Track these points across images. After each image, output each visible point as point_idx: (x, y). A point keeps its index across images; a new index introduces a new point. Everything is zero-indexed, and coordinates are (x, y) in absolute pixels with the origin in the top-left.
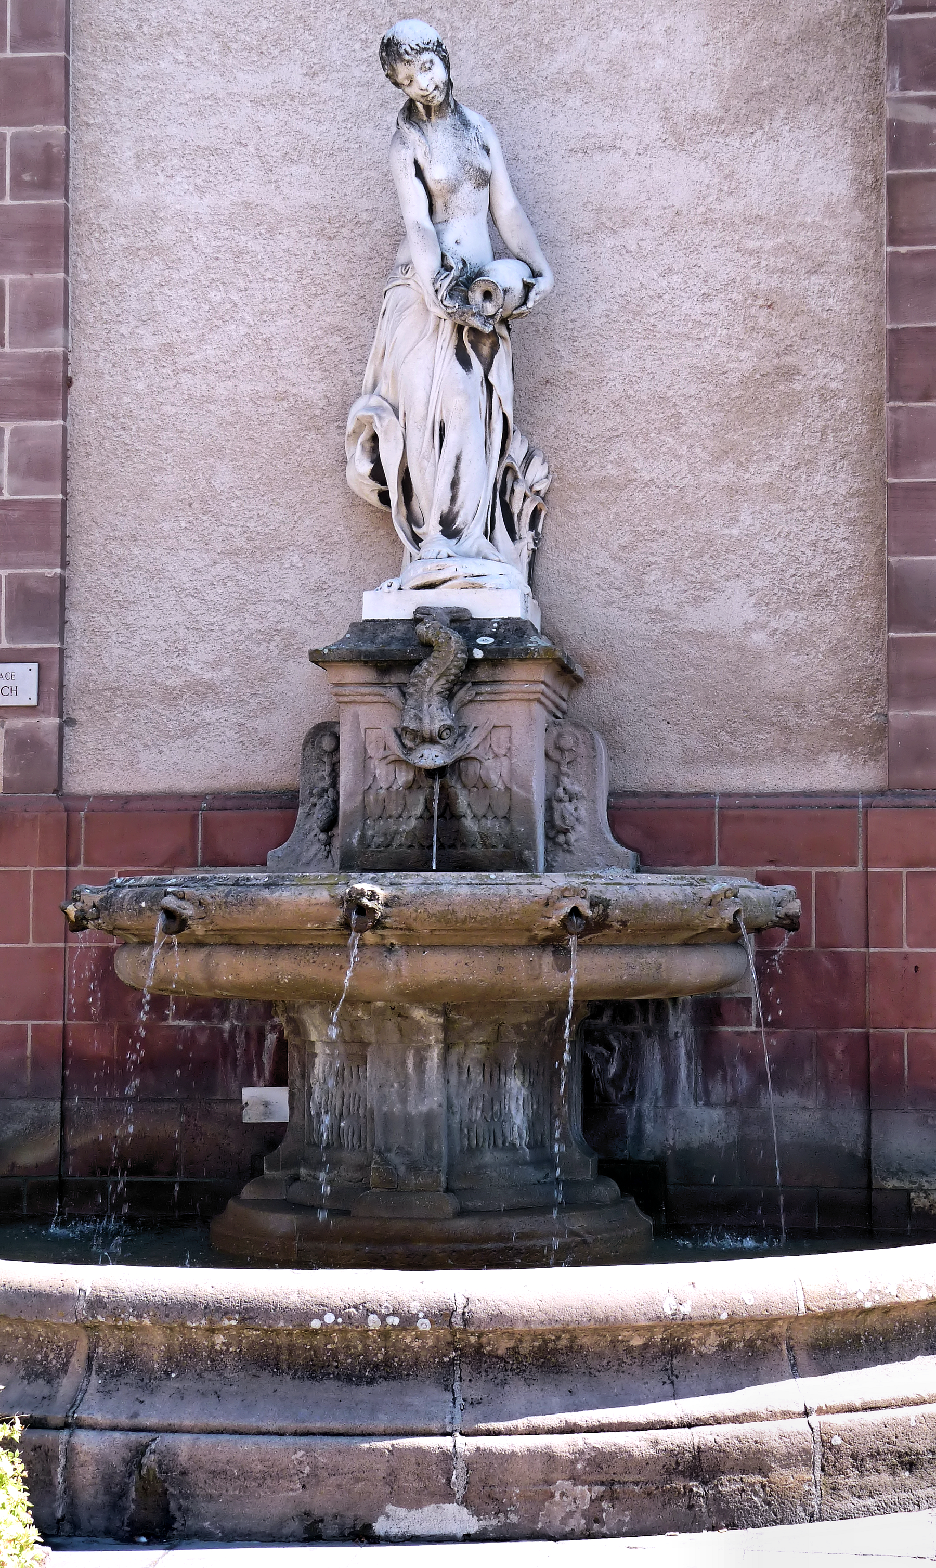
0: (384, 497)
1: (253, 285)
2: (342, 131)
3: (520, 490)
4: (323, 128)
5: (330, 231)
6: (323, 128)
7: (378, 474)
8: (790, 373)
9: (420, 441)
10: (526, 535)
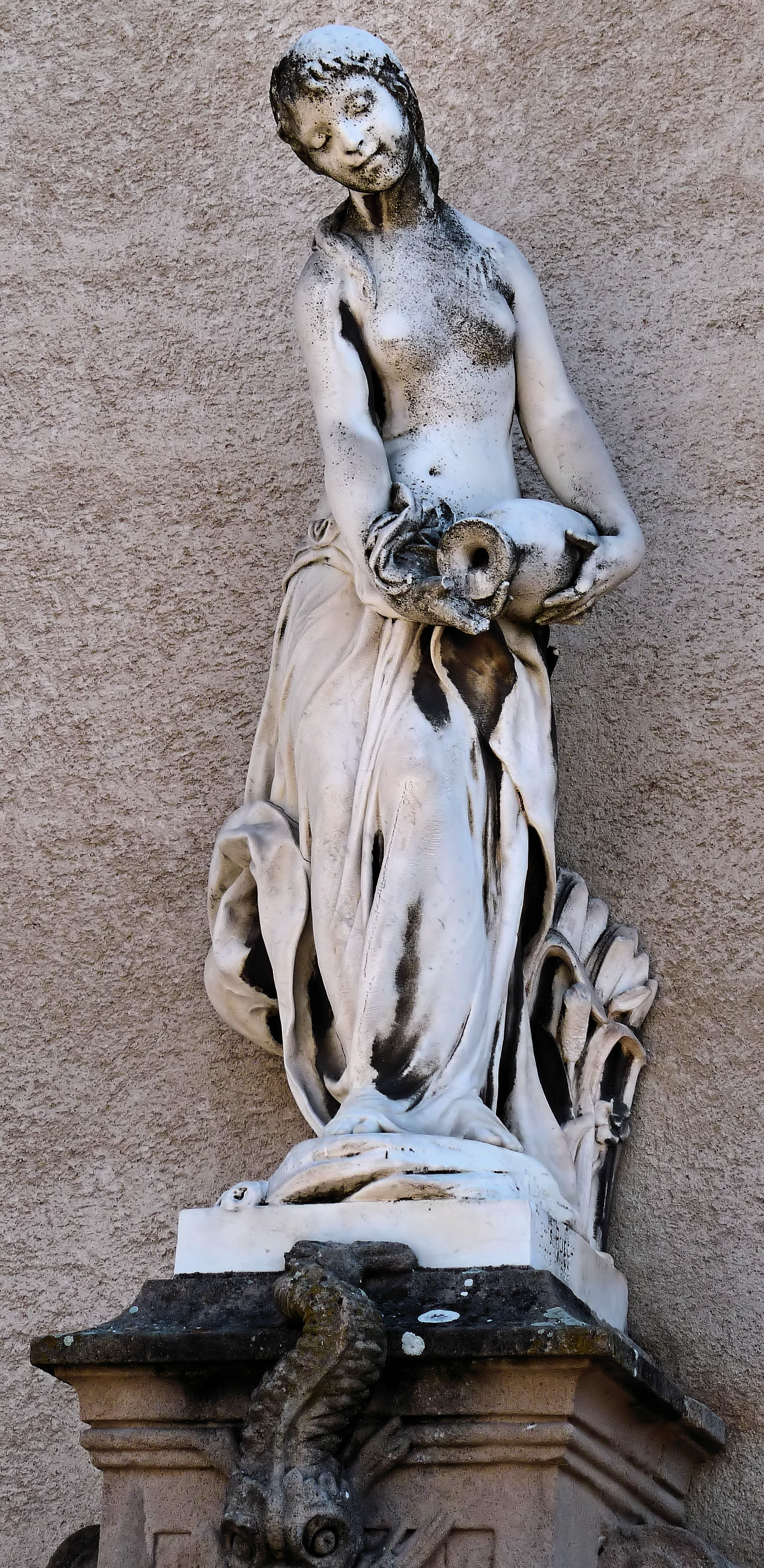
0: (273, 1021)
1: (63, 621)
2: (255, 323)
3: (577, 1007)
4: (220, 320)
5: (221, 509)
6: (220, 320)
7: (257, 971)
10: (593, 1109)
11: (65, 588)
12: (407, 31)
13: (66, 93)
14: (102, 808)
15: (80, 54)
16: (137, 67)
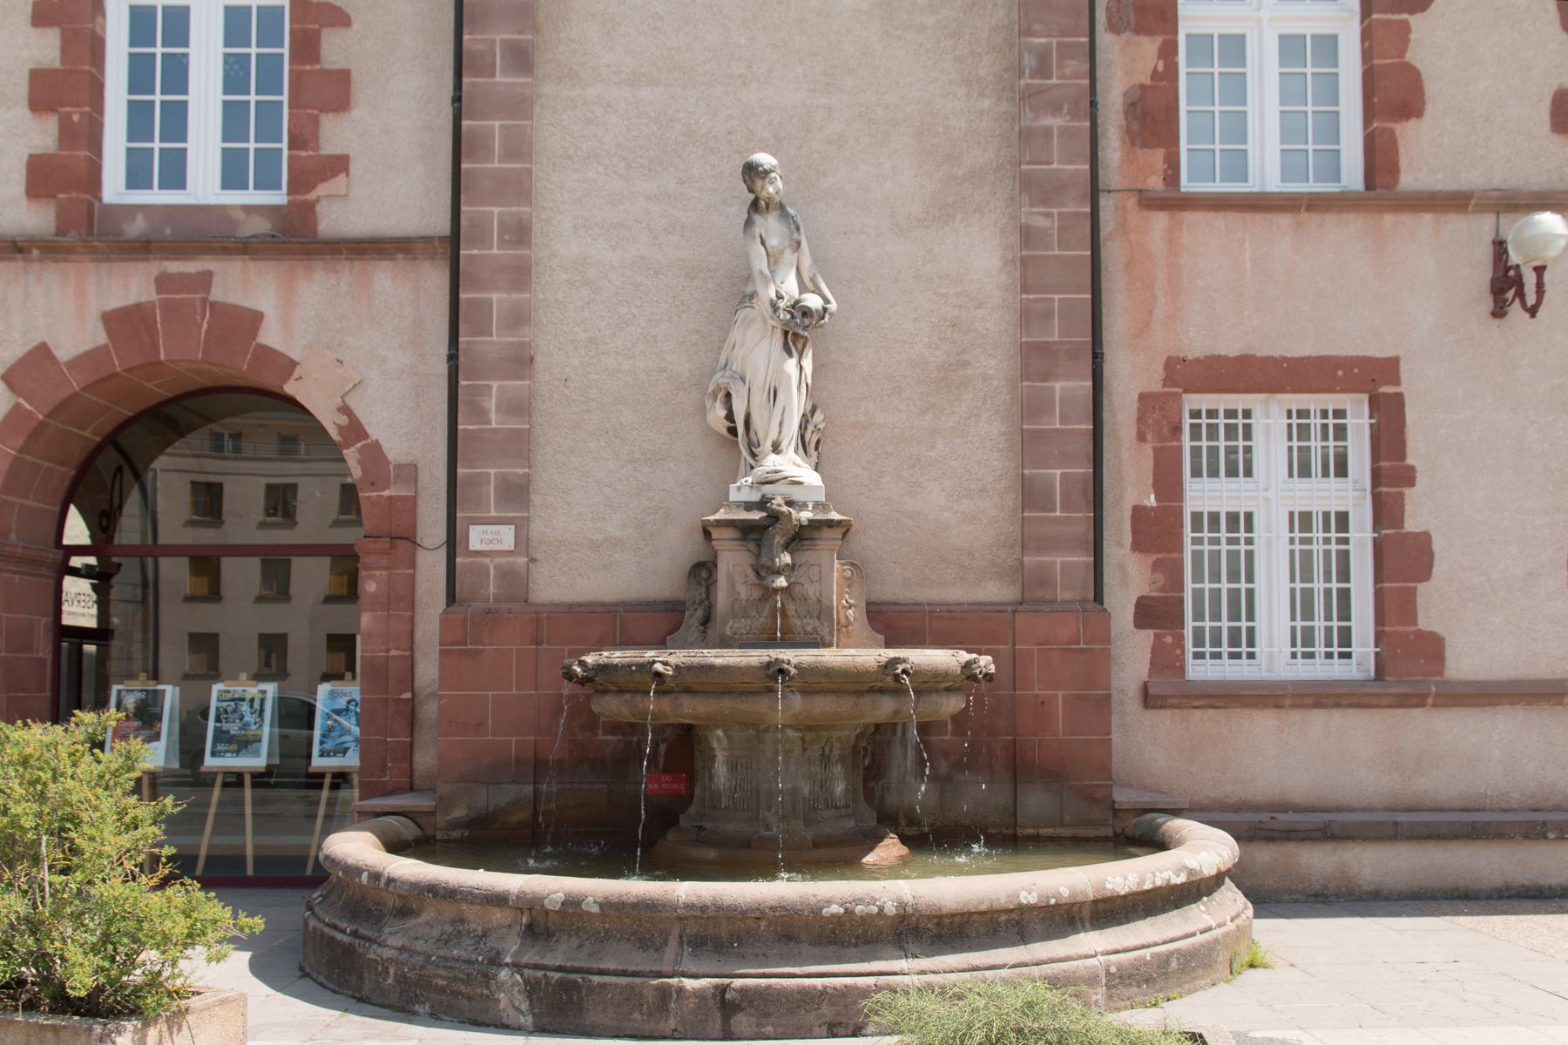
0: (733, 431)
3: (810, 428)
7: (730, 416)
8: (966, 364)
9: (759, 398)
10: (815, 454)
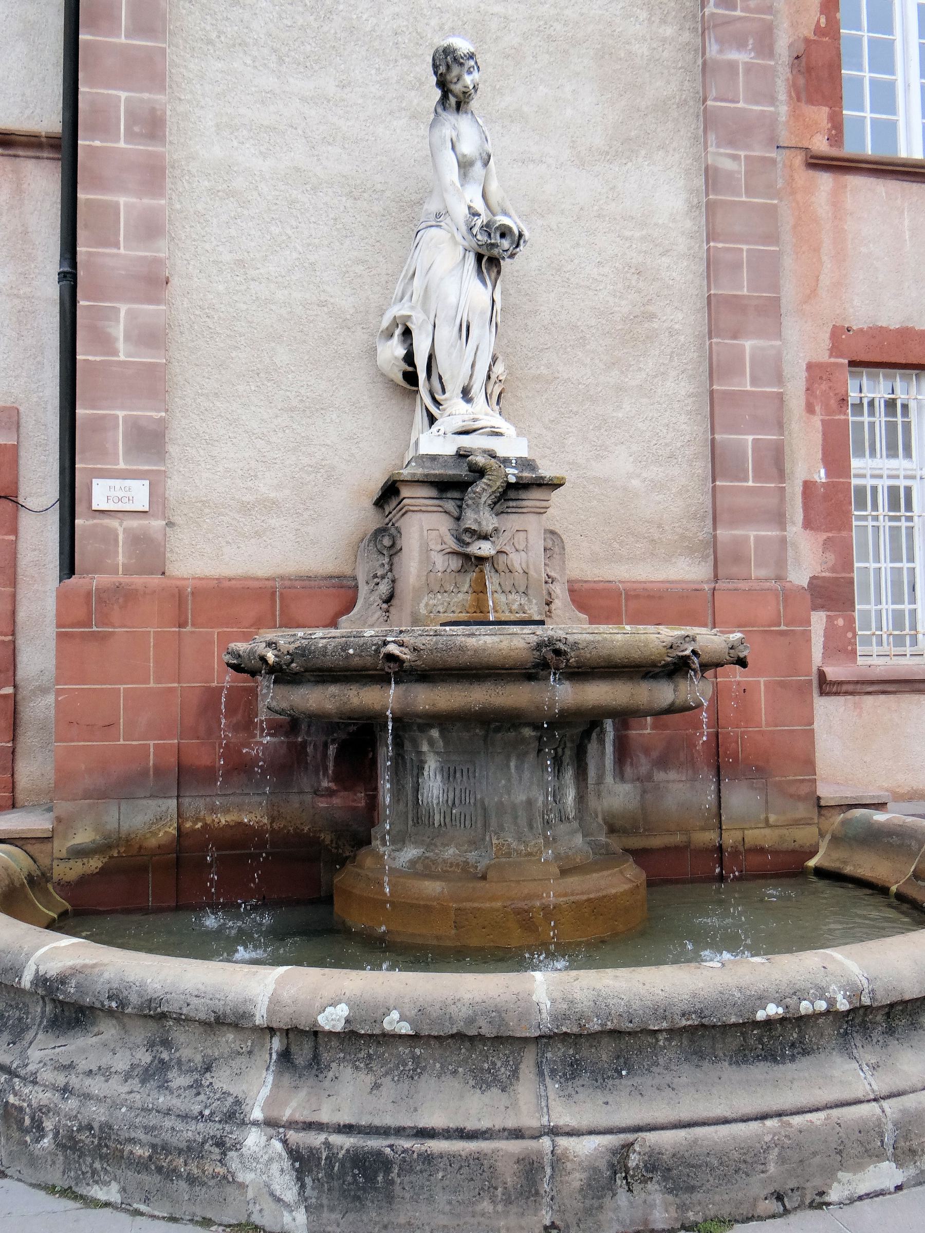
1: (303, 225)
2: (363, 128)
4: (350, 124)
5: (356, 194)
6: (350, 124)
7: (409, 358)
8: (652, 317)
9: (447, 333)
11: (302, 213)
12: (411, 30)
13: (285, 21)
14: (322, 294)
15: (290, 7)
16: (312, 18)
